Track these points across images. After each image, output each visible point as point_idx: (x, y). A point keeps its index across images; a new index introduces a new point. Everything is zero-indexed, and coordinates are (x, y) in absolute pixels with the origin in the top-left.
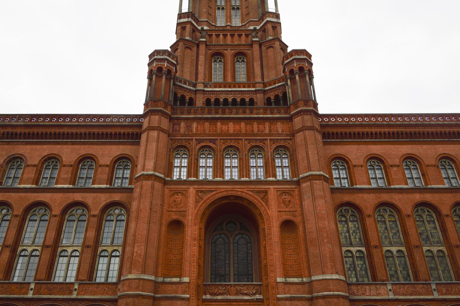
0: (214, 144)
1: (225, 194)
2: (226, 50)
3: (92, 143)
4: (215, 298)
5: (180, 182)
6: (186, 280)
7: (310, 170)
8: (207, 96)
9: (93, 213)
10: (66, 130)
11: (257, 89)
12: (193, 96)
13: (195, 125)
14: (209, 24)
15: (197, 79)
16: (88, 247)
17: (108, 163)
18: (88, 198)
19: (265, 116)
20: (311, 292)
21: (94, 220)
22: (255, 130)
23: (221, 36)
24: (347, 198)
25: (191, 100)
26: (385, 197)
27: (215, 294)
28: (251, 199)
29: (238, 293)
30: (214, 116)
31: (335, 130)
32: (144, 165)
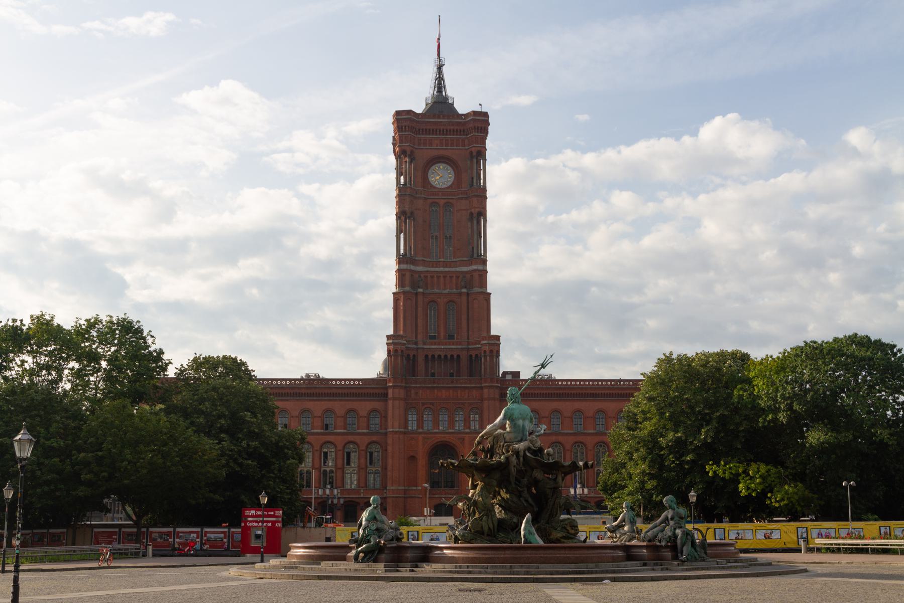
0: (433, 405)
1: (439, 440)
2: (440, 298)
4: (434, 496)
5: (412, 432)
9: (361, 448)
10: (334, 391)
11: (464, 347)
13: (420, 392)
14: (424, 263)
15: (416, 338)
16: (362, 469)
17: (366, 415)
18: (357, 439)
19: (466, 385)
21: (363, 453)
23: (435, 279)
25: (414, 356)
27: (434, 494)
30: (433, 385)
32: (393, 425)
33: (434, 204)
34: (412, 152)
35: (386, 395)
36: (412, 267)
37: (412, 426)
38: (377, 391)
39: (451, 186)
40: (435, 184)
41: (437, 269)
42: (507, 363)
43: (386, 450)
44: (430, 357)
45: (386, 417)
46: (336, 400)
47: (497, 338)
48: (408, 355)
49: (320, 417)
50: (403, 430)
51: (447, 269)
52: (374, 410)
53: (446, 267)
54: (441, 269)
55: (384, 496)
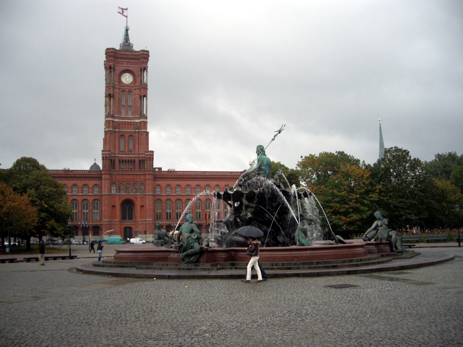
3: (86, 180)
6: (117, 220)
7: (149, 192)
8: (119, 158)
11: (137, 156)
12: (114, 158)
14: (119, 118)
15: (115, 151)
20: (146, 222)
22: (135, 178)
24: (159, 198)
25: (114, 160)
26: (169, 197)
28: (133, 200)
29: (129, 222)
31: (159, 176)
33: (124, 91)
34: (114, 67)
35: (101, 178)
36: (113, 120)
37: (114, 192)
38: (97, 176)
39: (131, 83)
40: (124, 82)
41: (125, 121)
42: (157, 164)
43: (102, 203)
44: (121, 160)
45: (101, 188)
46: (78, 180)
47: (153, 152)
48: (111, 160)
49: (70, 188)
50: (109, 194)
51: (129, 121)
52: (96, 185)
53: (129, 120)
54: (127, 121)
55: (101, 223)
